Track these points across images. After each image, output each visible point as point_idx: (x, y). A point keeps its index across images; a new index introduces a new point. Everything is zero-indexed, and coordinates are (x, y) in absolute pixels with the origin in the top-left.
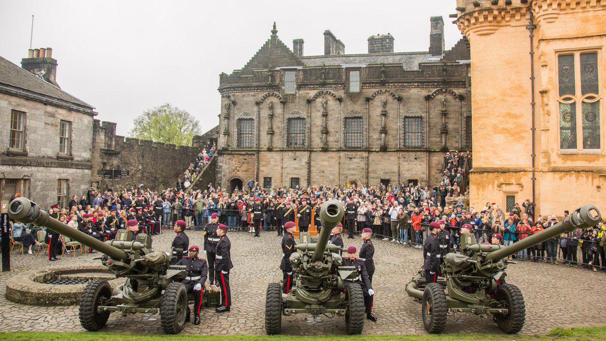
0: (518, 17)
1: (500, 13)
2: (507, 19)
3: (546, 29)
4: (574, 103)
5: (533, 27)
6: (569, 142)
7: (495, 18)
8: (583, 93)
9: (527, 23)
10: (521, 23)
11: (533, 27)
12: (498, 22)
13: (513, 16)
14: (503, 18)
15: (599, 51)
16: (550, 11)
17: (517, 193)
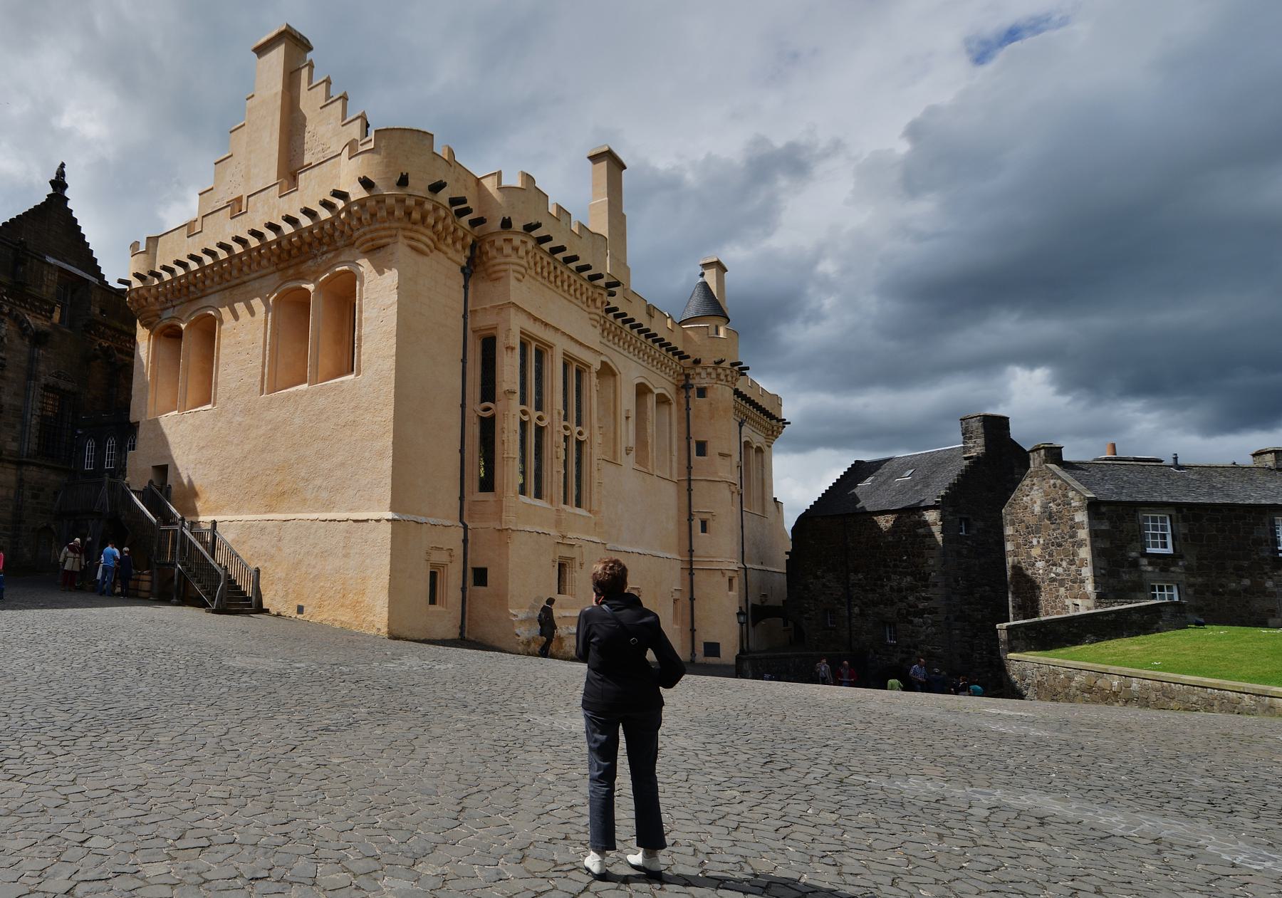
9: (464, 262)
16: (524, 262)
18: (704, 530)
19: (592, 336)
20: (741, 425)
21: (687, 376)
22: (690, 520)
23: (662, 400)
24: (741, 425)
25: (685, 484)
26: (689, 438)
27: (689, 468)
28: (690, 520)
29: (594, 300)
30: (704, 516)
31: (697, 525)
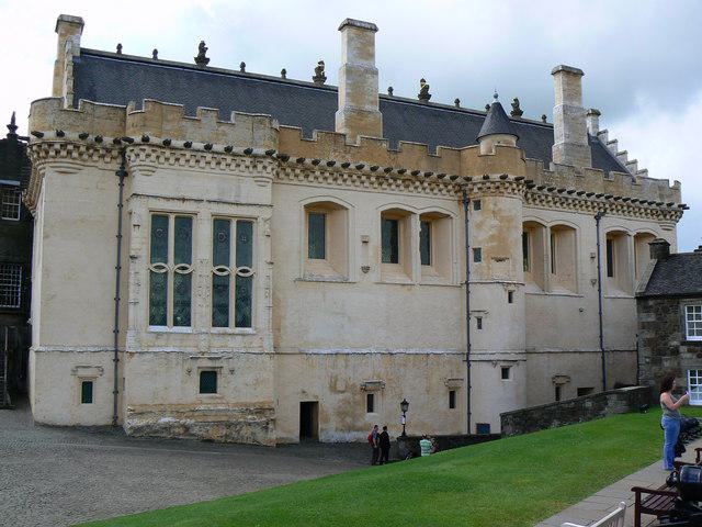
1: (88, 149)
2: (95, 158)
3: (140, 182)
4: (166, 273)
5: (123, 174)
6: (157, 318)
7: (81, 154)
8: (176, 263)
9: (116, 166)
11: (123, 174)
12: (84, 161)
13: (103, 156)
14: (91, 156)
15: (195, 217)
16: (148, 162)
18: (480, 327)
19: (264, 194)
20: (598, 218)
21: (465, 194)
22: (468, 319)
23: (429, 220)
24: (598, 218)
25: (464, 287)
26: (468, 247)
27: (468, 272)
28: (468, 319)
29: (255, 167)
30: (477, 314)
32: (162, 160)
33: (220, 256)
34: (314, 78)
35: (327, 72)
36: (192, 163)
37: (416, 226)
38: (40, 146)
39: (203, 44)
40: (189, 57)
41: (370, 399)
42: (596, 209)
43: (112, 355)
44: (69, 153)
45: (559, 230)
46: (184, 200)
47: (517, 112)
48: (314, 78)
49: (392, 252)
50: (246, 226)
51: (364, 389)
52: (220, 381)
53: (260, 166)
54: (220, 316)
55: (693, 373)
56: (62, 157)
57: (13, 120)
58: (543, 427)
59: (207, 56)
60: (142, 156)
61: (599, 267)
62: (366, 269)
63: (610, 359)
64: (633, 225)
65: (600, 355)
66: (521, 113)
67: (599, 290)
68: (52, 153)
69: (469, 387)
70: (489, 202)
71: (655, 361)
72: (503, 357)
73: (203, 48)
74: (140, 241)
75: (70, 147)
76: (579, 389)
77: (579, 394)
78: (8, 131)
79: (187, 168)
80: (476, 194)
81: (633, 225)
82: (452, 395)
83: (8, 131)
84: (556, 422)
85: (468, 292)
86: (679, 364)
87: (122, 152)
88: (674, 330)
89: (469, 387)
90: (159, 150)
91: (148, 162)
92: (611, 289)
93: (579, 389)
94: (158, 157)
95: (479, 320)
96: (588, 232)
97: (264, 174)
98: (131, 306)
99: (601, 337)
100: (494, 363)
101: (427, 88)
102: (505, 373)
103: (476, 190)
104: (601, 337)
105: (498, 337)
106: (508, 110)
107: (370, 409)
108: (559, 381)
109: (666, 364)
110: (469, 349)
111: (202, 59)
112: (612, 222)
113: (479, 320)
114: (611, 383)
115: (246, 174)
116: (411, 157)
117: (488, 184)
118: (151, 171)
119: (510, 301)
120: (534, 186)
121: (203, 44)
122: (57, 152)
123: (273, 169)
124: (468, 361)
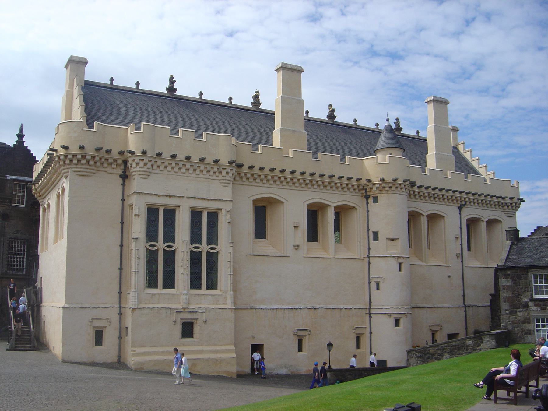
0: (114, 166)
4: (157, 250)
5: (125, 177)
6: (151, 282)
7: (95, 163)
8: (165, 242)
9: (121, 172)
10: (115, 171)
11: (125, 177)
12: (98, 167)
13: (111, 164)
16: (145, 169)
17: (105, 327)
18: (378, 289)
19: (226, 193)
20: (460, 208)
21: (366, 190)
22: (370, 283)
24: (460, 208)
26: (368, 230)
27: (369, 249)
28: (370, 283)
29: (220, 173)
31: (373, 286)
32: (155, 167)
33: (195, 238)
34: (252, 103)
35: (261, 99)
36: (176, 169)
37: (331, 215)
38: (66, 156)
39: (172, 78)
40: (162, 89)
41: (300, 341)
42: (459, 202)
43: (118, 310)
44: (88, 161)
45: (433, 218)
46: (170, 196)
47: (399, 129)
48: (252, 103)
49: (313, 235)
50: (213, 216)
51: (295, 333)
52: (197, 329)
53: (224, 173)
54: (195, 283)
55: (538, 321)
56: (82, 165)
57: (21, 130)
58: (439, 359)
59: (175, 86)
60: (142, 164)
61: (461, 245)
62: (297, 248)
63: (470, 312)
64: (486, 214)
65: (464, 309)
66: (401, 129)
67: (462, 261)
68: (75, 161)
69: (371, 333)
70: (383, 198)
71: (513, 313)
72: (396, 311)
73: (172, 81)
74: (138, 227)
75: (88, 157)
76: (448, 334)
77: (449, 339)
78: (17, 139)
79: (172, 173)
80: (374, 191)
81: (486, 214)
82: (358, 338)
83: (17, 139)
84: (447, 355)
85: (369, 263)
86: (528, 314)
87: (125, 162)
88: (525, 291)
89: (371, 333)
90: (153, 160)
91: (145, 169)
92: (471, 262)
93: (448, 334)
94: (152, 166)
95: (378, 284)
96: (453, 221)
97: (227, 178)
98: (133, 274)
99: (464, 296)
100: (389, 315)
101: (333, 111)
102: (397, 323)
103: (374, 189)
104: (464, 296)
105: (390, 297)
106: (394, 126)
107: (300, 350)
108: (434, 328)
109: (520, 314)
110: (370, 305)
111: (171, 89)
112: (470, 212)
113: (378, 284)
114: (471, 330)
115: (214, 177)
116: (328, 163)
117: (384, 185)
118: (147, 175)
119: (400, 270)
120: (415, 185)
121: (172, 78)
122: (79, 161)
123: (233, 174)
124: (370, 314)
